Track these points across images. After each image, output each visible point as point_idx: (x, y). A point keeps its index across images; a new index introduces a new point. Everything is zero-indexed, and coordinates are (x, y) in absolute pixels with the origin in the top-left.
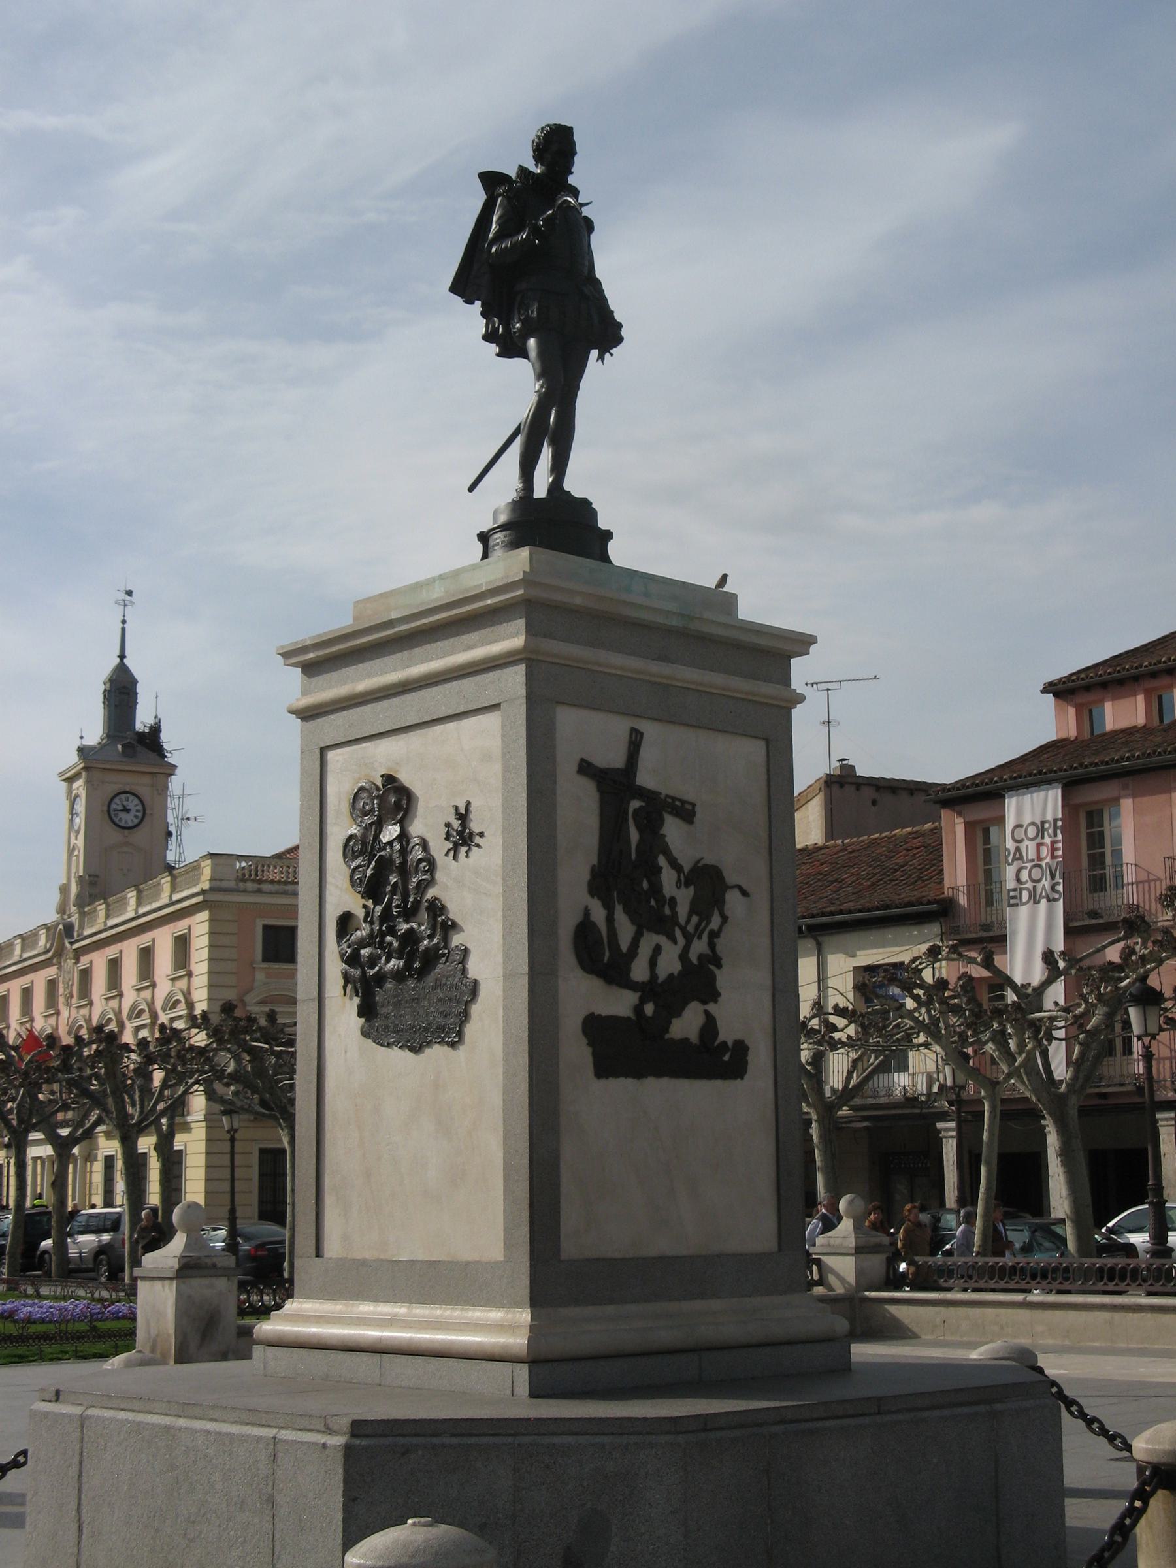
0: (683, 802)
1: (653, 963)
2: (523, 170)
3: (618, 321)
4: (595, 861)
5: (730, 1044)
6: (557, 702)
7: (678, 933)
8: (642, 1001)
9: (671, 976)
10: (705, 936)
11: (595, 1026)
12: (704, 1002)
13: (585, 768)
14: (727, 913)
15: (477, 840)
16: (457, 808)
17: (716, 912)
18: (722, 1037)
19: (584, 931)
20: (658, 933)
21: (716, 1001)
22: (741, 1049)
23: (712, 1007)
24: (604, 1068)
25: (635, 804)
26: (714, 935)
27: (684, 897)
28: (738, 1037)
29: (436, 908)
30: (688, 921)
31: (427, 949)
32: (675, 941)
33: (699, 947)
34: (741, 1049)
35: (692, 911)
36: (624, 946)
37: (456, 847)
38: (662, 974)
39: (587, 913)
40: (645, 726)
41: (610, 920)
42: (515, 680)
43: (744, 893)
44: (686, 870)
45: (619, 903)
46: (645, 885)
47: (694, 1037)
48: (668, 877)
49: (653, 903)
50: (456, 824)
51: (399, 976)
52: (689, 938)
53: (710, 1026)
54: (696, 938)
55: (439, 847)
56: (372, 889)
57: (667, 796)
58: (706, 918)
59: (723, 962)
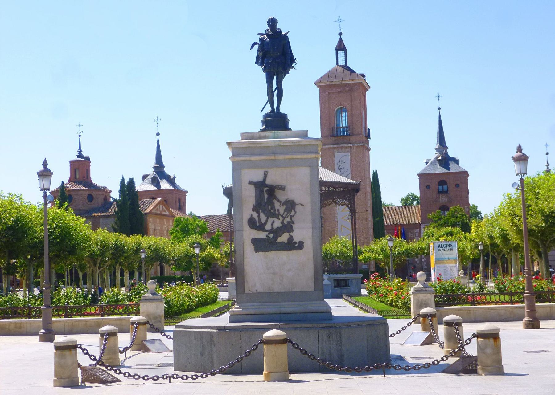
0: (281, 186)
1: (272, 225)
5: (298, 242)
7: (280, 217)
10: (289, 217)
13: (250, 183)
18: (294, 240)
20: (273, 218)
23: (291, 234)
25: (266, 189)
26: (292, 217)
27: (282, 209)
30: (284, 214)
33: (288, 219)
35: (285, 212)
36: (263, 222)
39: (252, 215)
41: (259, 216)
43: (302, 205)
44: (283, 202)
47: (286, 241)
52: (284, 218)
54: (286, 218)
57: (276, 185)
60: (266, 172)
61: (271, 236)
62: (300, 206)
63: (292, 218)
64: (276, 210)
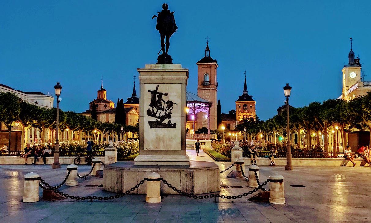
1: (160, 114)
11: (150, 123)
13: (149, 91)
23: (170, 119)
24: (151, 127)
25: (158, 94)
26: (170, 110)
27: (165, 106)
32: (164, 111)
33: (168, 112)
38: (161, 115)
39: (149, 108)
41: (153, 109)
47: (167, 123)
52: (166, 111)
53: (170, 122)
58: (170, 107)
61: (159, 120)
64: (162, 106)
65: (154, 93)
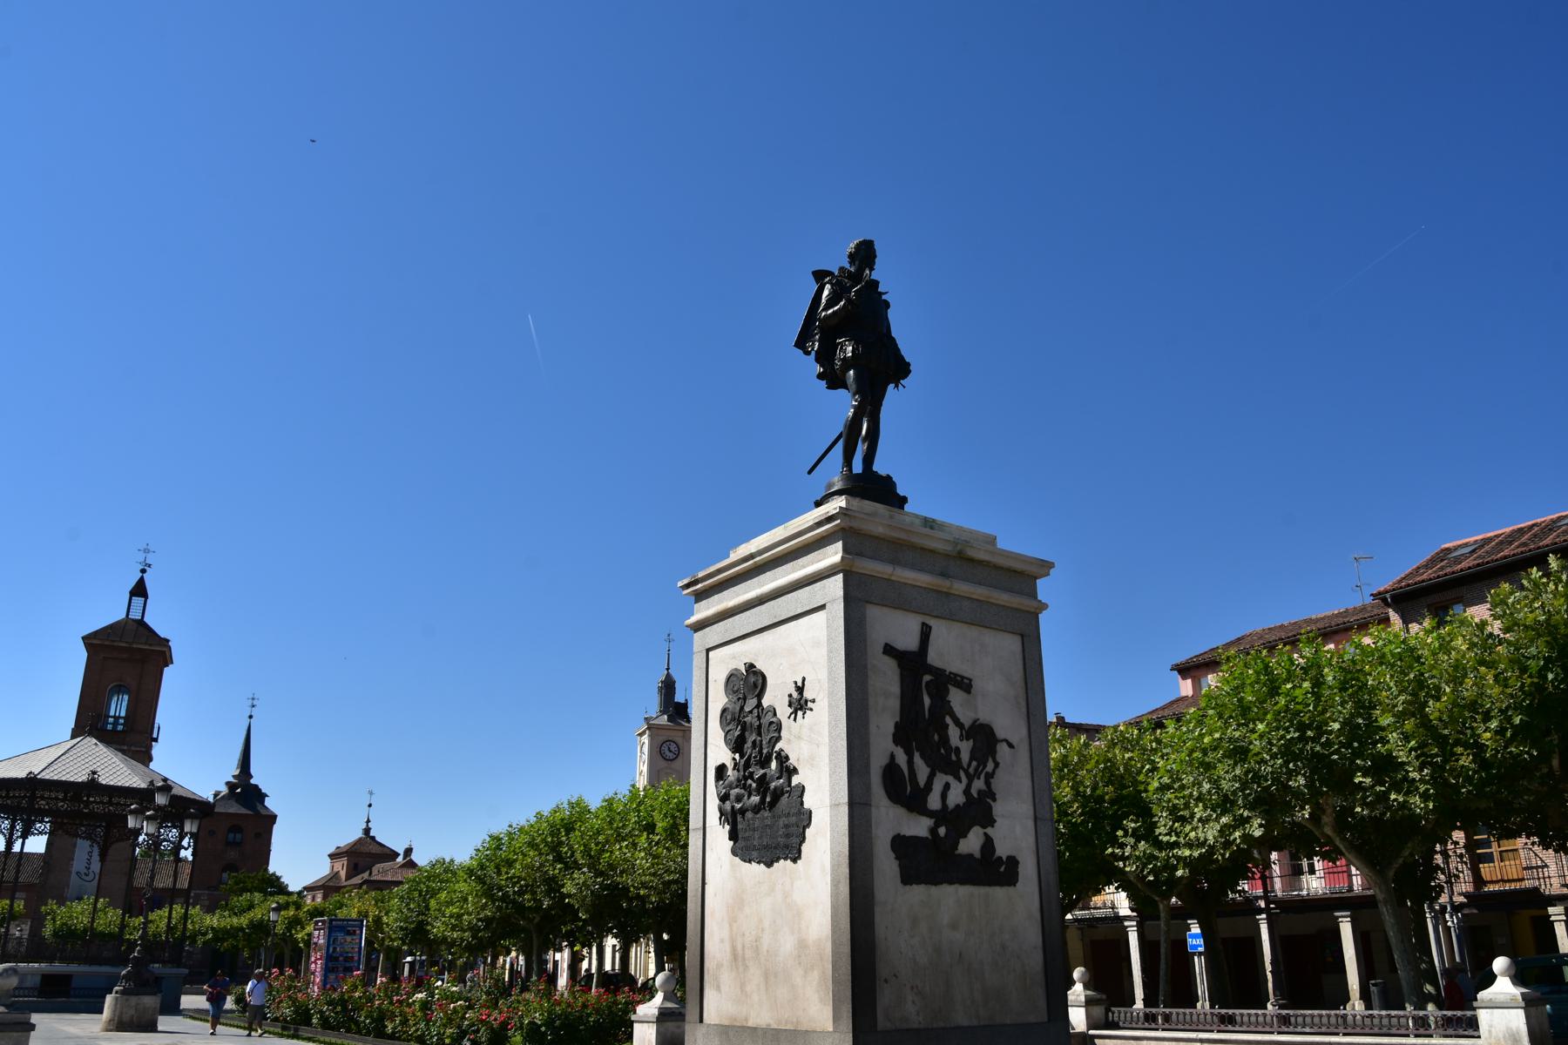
0: (963, 677)
1: (944, 796)
2: (842, 269)
3: (907, 361)
4: (898, 719)
5: (1004, 859)
6: (867, 602)
7: (962, 774)
8: (937, 825)
9: (958, 806)
10: (982, 776)
11: (901, 844)
12: (984, 827)
13: (889, 650)
14: (998, 759)
15: (810, 704)
16: (796, 683)
17: (990, 760)
19: (891, 771)
21: (993, 826)
22: (1013, 862)
23: (989, 830)
24: (908, 878)
25: (927, 678)
26: (990, 776)
27: (966, 748)
28: (1013, 853)
29: (783, 759)
30: (969, 765)
31: (776, 788)
32: (961, 782)
33: (979, 784)
34: (1013, 862)
35: (972, 759)
37: (795, 712)
39: (892, 756)
40: (931, 622)
41: (910, 762)
42: (836, 585)
43: (1011, 746)
44: (967, 726)
45: (917, 751)
46: (936, 737)
47: (977, 855)
48: (954, 733)
49: (943, 751)
50: (795, 695)
51: (757, 809)
52: (970, 779)
53: (988, 844)
54: (976, 780)
55: (783, 712)
56: (737, 746)
57: (950, 673)
59: (997, 796)
60: (927, 625)
62: (1005, 744)
63: (992, 780)
65: (912, 664)
